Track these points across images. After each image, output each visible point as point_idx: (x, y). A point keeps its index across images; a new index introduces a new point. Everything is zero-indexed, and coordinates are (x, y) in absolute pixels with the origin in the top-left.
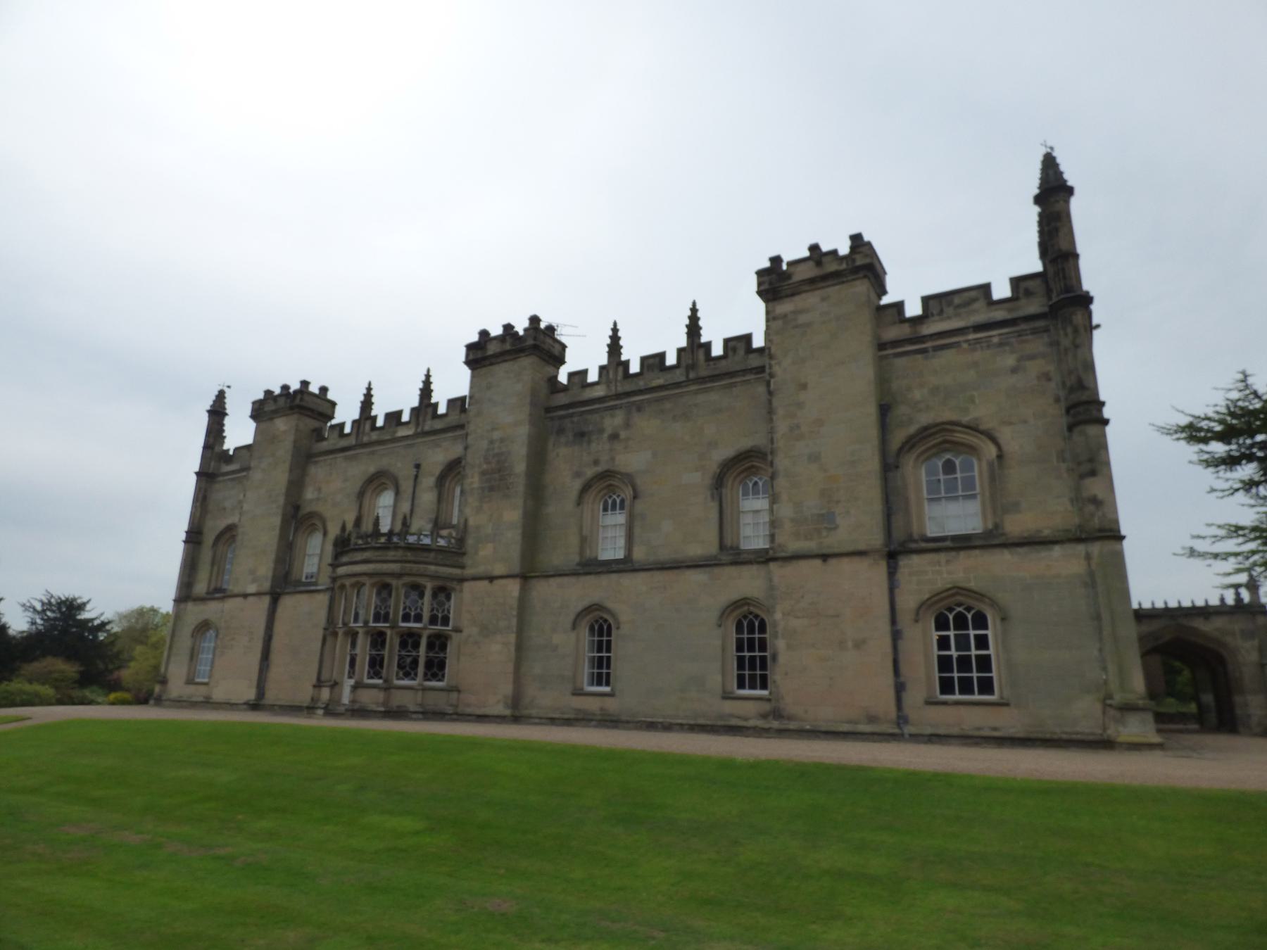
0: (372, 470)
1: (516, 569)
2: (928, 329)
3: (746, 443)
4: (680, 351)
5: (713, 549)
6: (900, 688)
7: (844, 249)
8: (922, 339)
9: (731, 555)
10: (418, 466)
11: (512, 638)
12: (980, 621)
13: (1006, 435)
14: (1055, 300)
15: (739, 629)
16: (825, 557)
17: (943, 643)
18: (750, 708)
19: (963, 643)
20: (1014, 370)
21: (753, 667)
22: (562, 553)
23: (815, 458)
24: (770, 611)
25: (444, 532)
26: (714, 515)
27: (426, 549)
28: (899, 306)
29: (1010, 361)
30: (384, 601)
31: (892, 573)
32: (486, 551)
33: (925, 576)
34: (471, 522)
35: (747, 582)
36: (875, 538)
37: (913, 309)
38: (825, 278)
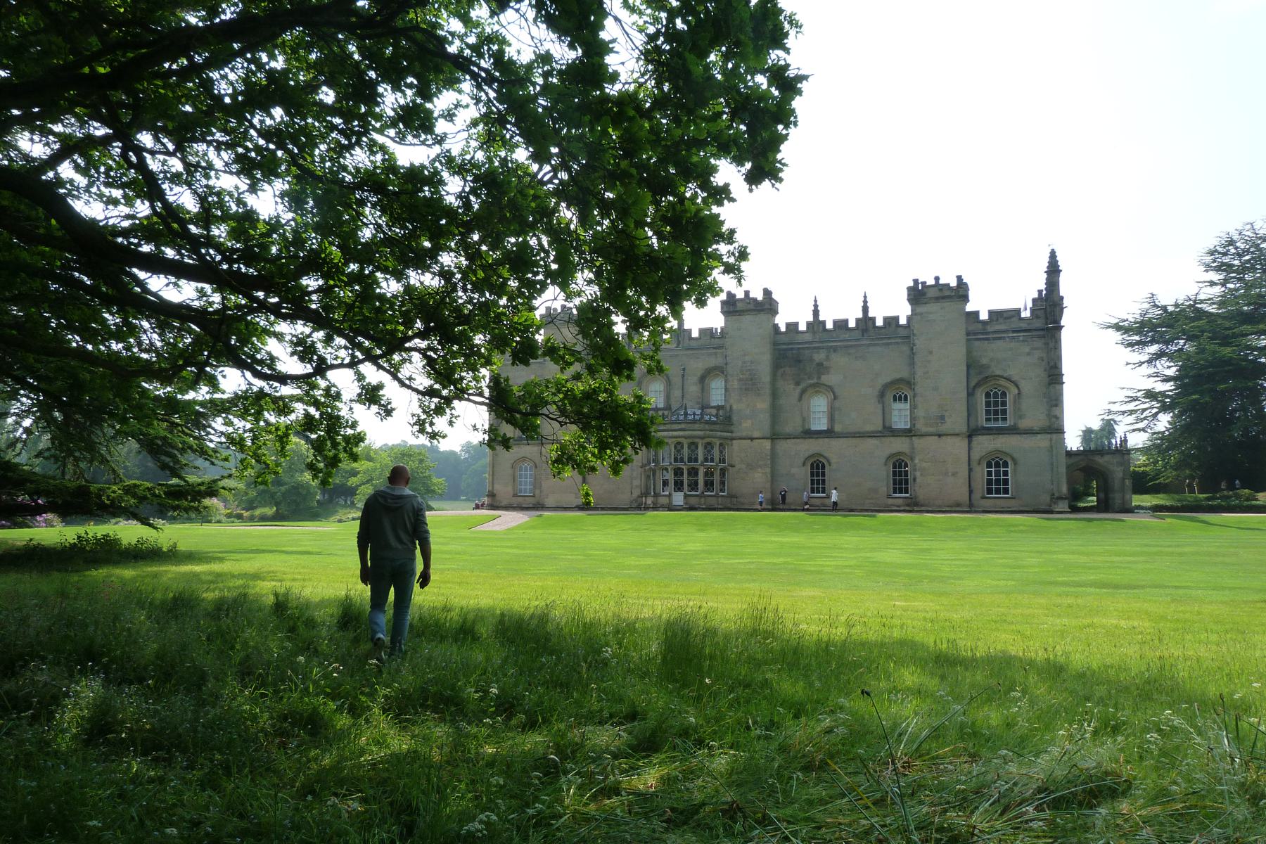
1: (767, 432)
2: (990, 329)
3: (898, 376)
5: (880, 428)
6: (971, 492)
7: (954, 284)
8: (988, 333)
9: (889, 431)
11: (768, 470)
12: (1006, 464)
13: (1022, 384)
14: (1050, 305)
15: (894, 467)
16: (940, 436)
17: (989, 473)
18: (900, 501)
19: (997, 474)
20: (1028, 354)
21: (900, 483)
22: (791, 425)
23: (936, 389)
24: (912, 459)
25: (708, 411)
26: (880, 412)
27: (714, 423)
28: (976, 313)
29: (1027, 350)
30: (679, 451)
31: (970, 443)
32: (747, 424)
33: (985, 444)
34: (735, 407)
35: (900, 445)
36: (964, 429)
37: (984, 316)
38: (944, 298)
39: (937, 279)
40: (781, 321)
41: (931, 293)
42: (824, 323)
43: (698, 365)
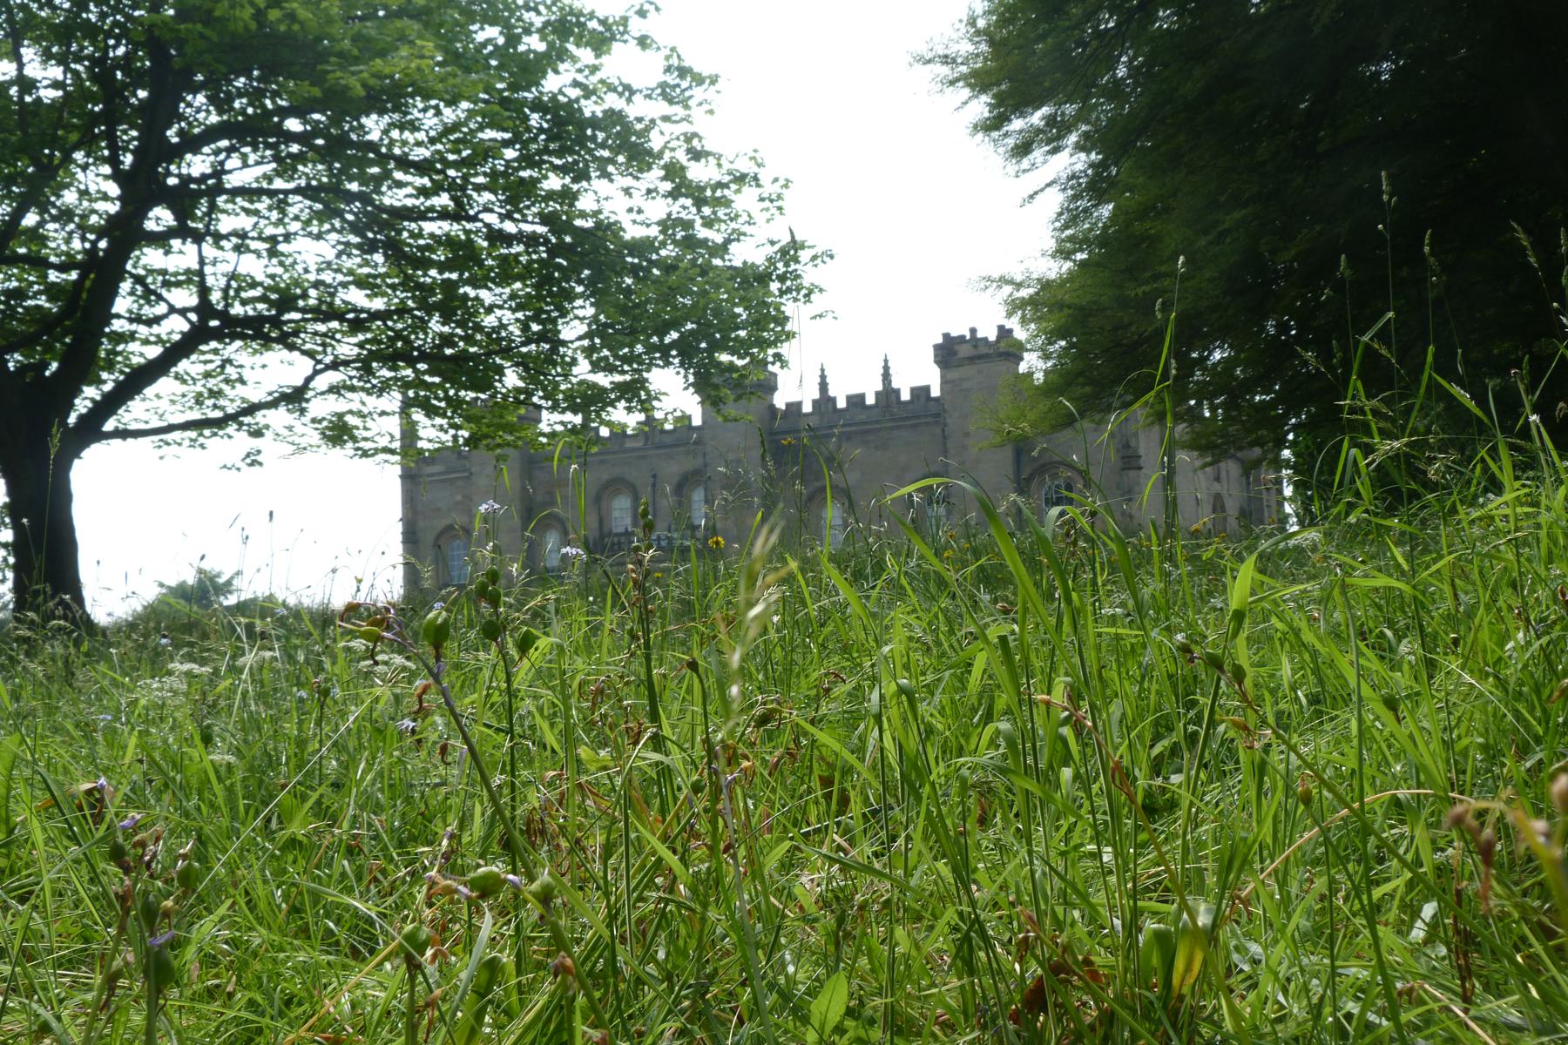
0: (605, 477)
4: (878, 394)
10: (654, 476)
38: (980, 357)
39: (973, 331)
40: (780, 401)
41: (964, 351)
42: (834, 400)
43: (673, 469)
